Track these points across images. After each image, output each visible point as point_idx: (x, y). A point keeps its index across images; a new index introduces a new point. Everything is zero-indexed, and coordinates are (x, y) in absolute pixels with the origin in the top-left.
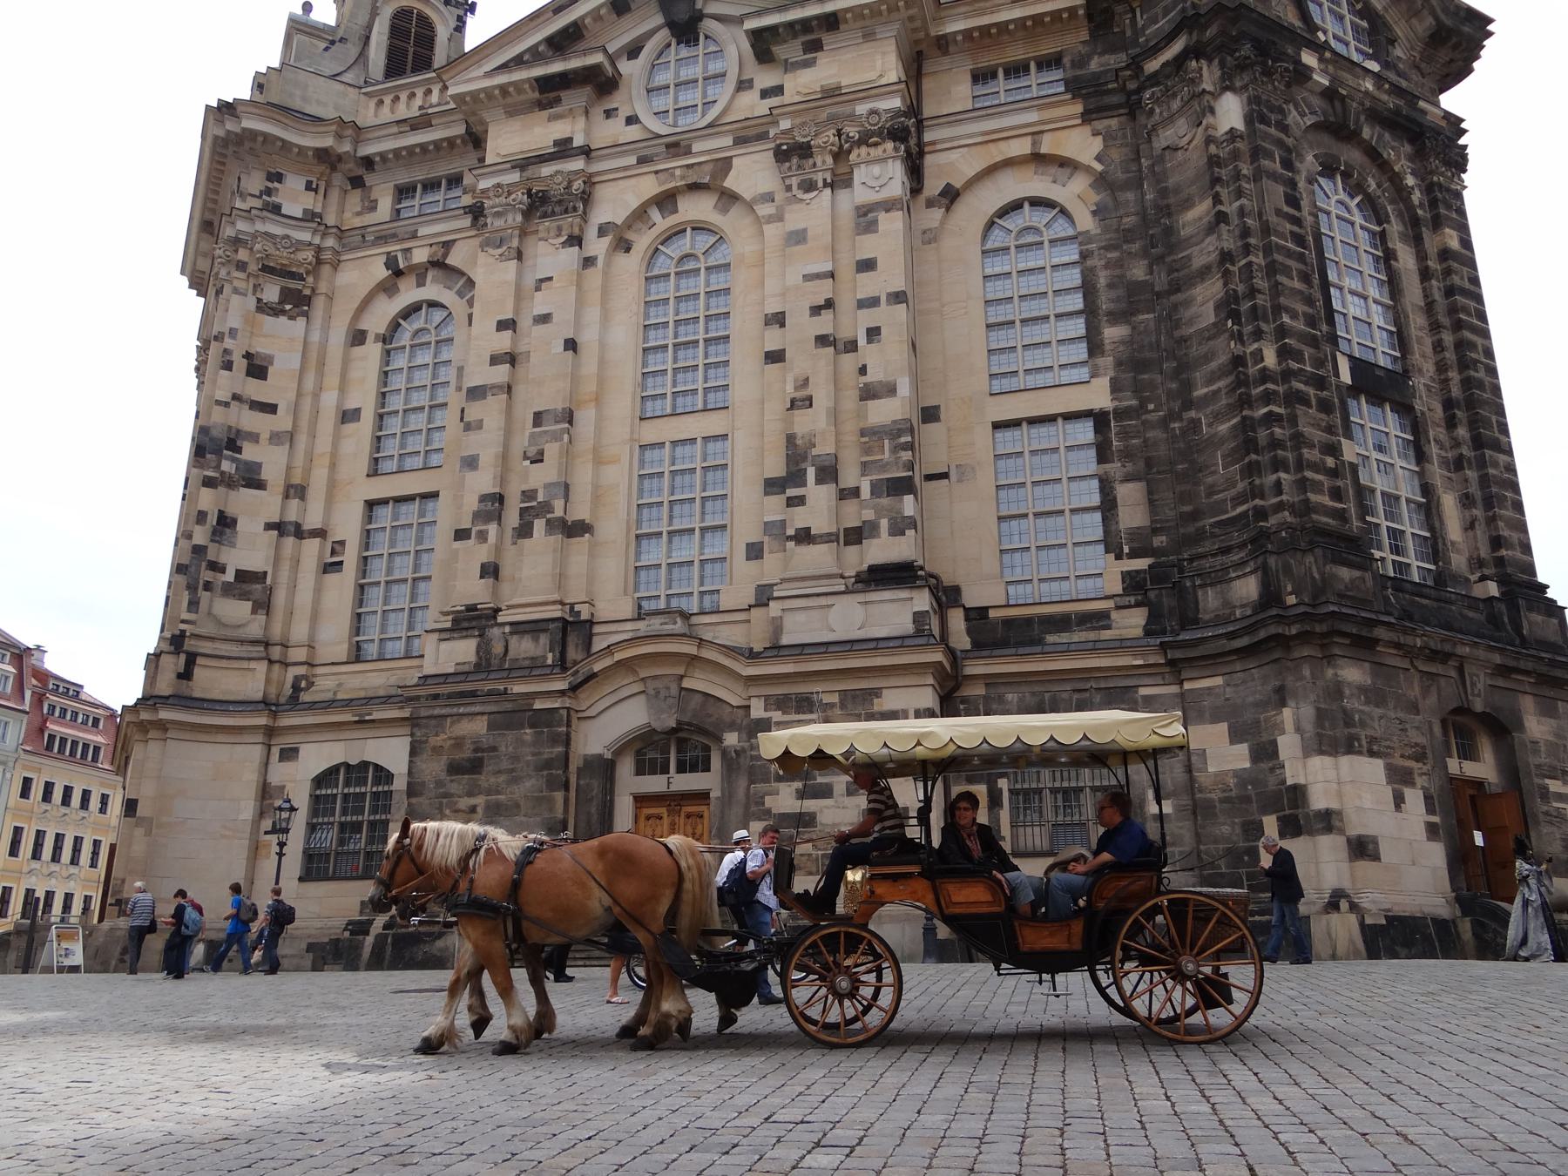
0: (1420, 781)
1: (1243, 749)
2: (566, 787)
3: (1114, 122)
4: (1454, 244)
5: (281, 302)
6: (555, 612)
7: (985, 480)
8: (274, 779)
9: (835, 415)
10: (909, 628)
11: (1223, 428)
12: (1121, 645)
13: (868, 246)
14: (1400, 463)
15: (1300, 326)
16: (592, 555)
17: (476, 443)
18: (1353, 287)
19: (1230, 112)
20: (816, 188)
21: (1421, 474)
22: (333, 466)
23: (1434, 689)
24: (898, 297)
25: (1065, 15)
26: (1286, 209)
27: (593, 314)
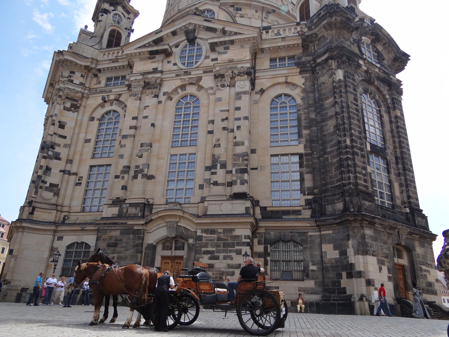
0: (387, 264)
1: (337, 252)
2: (142, 252)
3: (308, 75)
4: (399, 114)
5: (71, 107)
6: (142, 201)
7: (268, 171)
8: (55, 246)
9: (226, 149)
10: (244, 212)
11: (335, 160)
12: (304, 220)
13: (238, 104)
14: (383, 173)
15: (357, 134)
17: (123, 151)
18: (372, 124)
19: (340, 75)
20: (225, 87)
21: (389, 177)
22: (81, 155)
23: (391, 238)
24: (246, 118)
25: (296, 45)
27: (160, 117)
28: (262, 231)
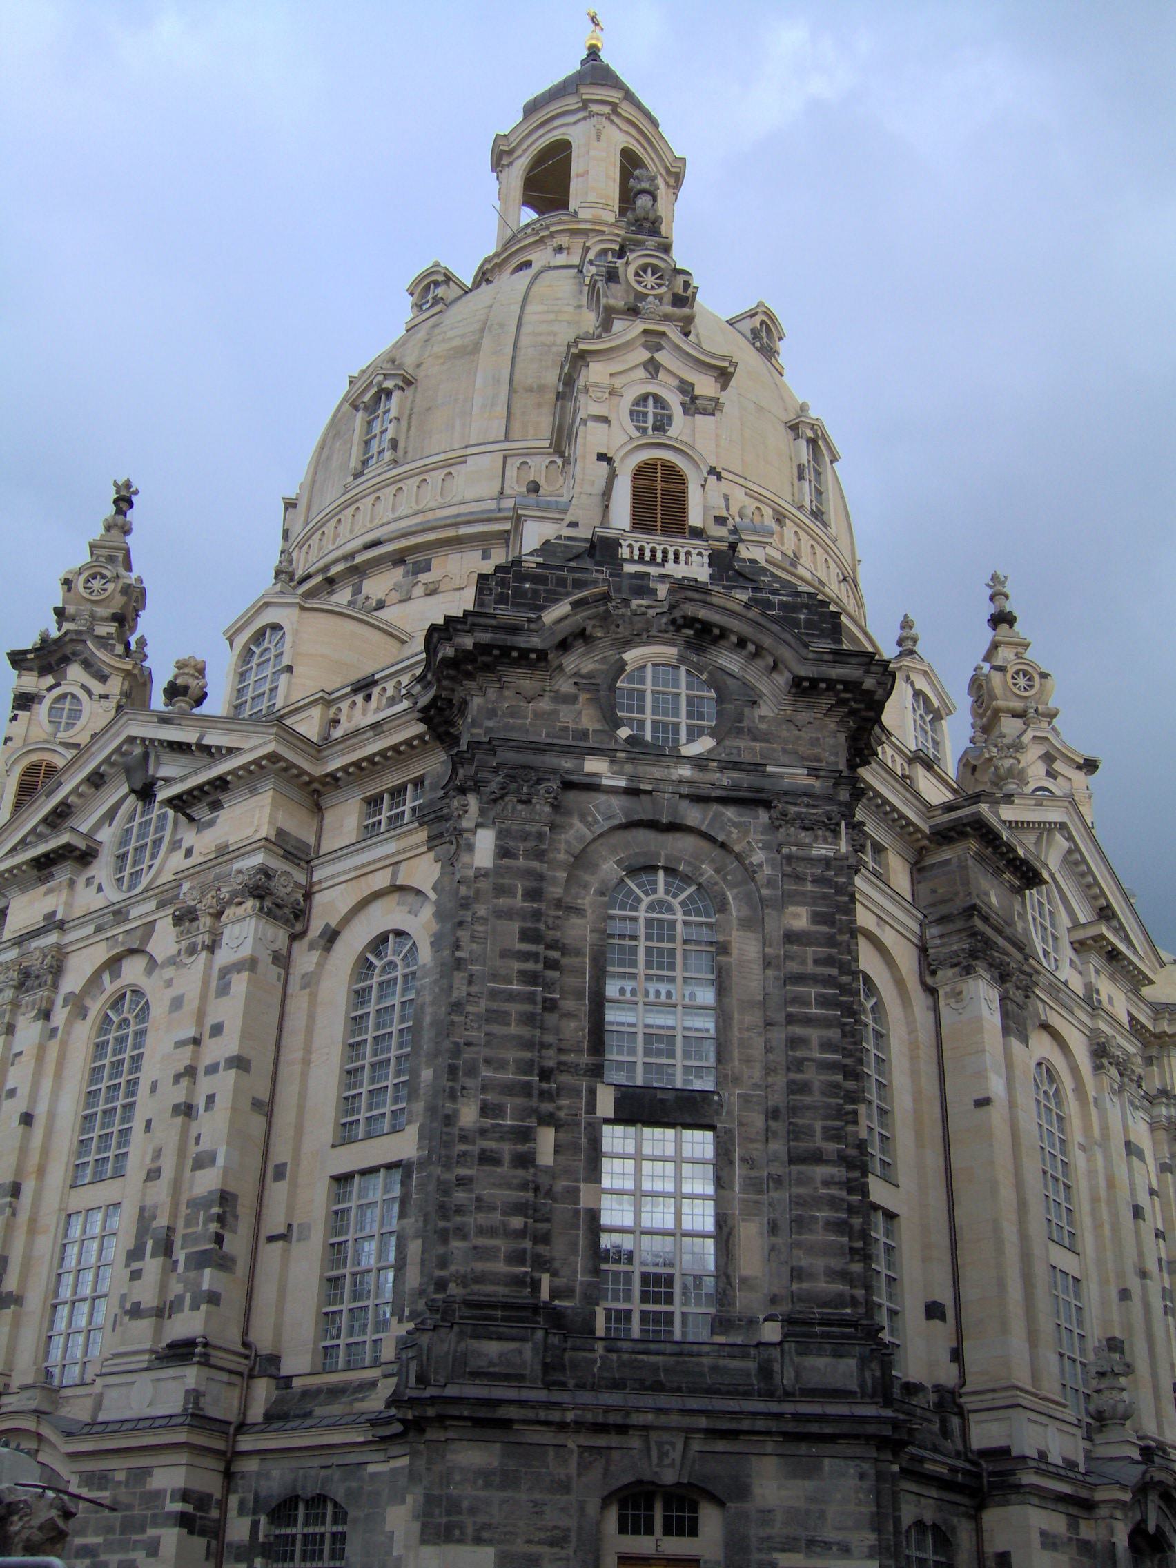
15: (511, 1076)
19: (484, 847)
24: (240, 1063)
27: (47, 1085)
28: (251, 1465)
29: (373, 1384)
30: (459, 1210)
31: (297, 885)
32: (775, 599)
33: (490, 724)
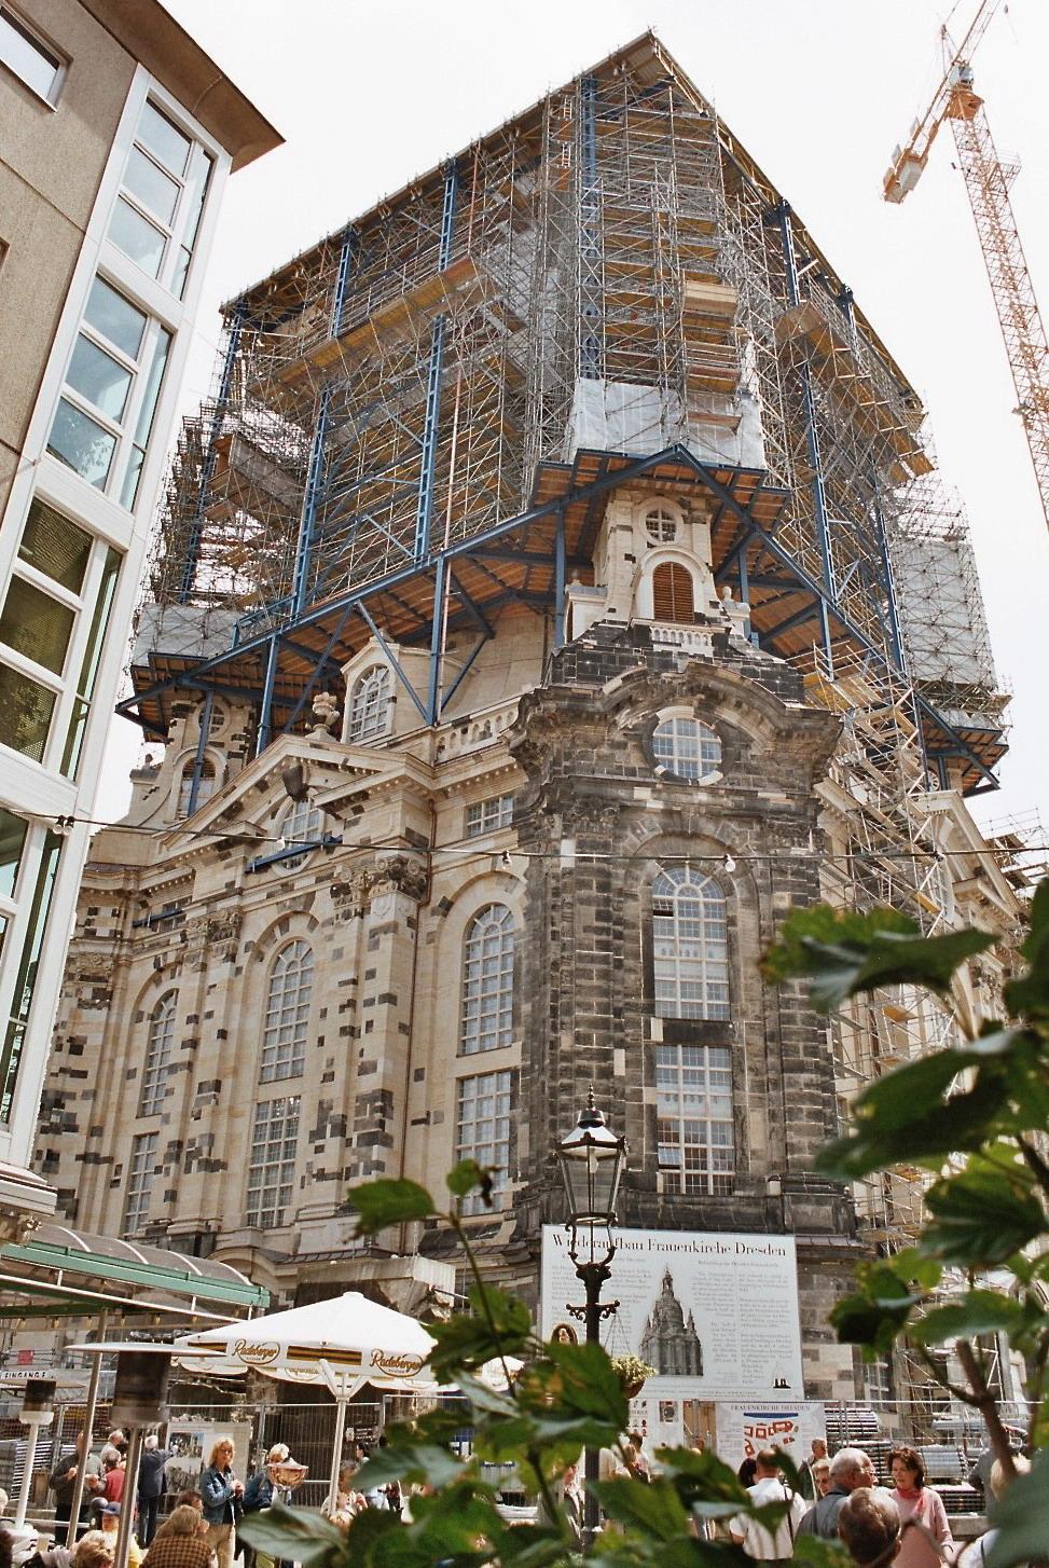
5: (94, 998)
6: (192, 1227)
13: (372, 960)
16: (224, 1182)
22: (119, 1110)
24: (390, 998)
26: (596, 924)
29: (497, 1226)
30: (564, 1108)
31: (421, 869)
32: (759, 669)
33: (564, 763)
